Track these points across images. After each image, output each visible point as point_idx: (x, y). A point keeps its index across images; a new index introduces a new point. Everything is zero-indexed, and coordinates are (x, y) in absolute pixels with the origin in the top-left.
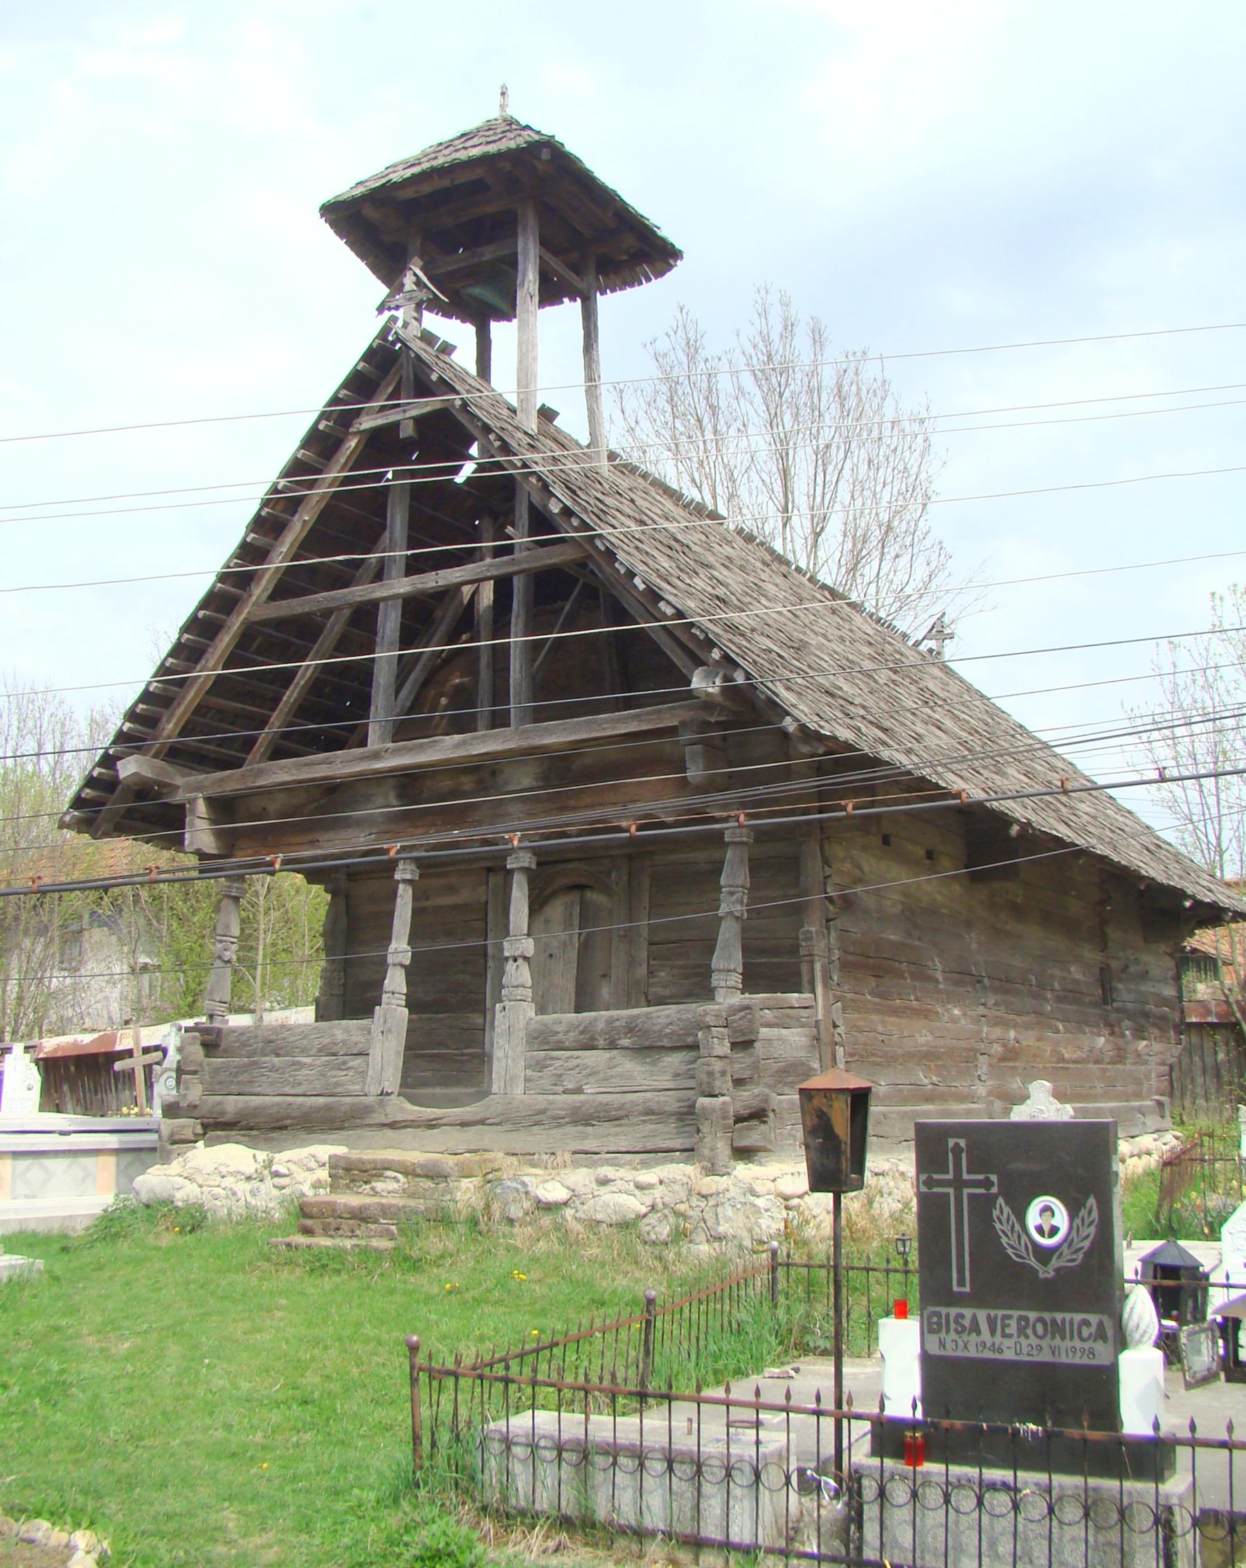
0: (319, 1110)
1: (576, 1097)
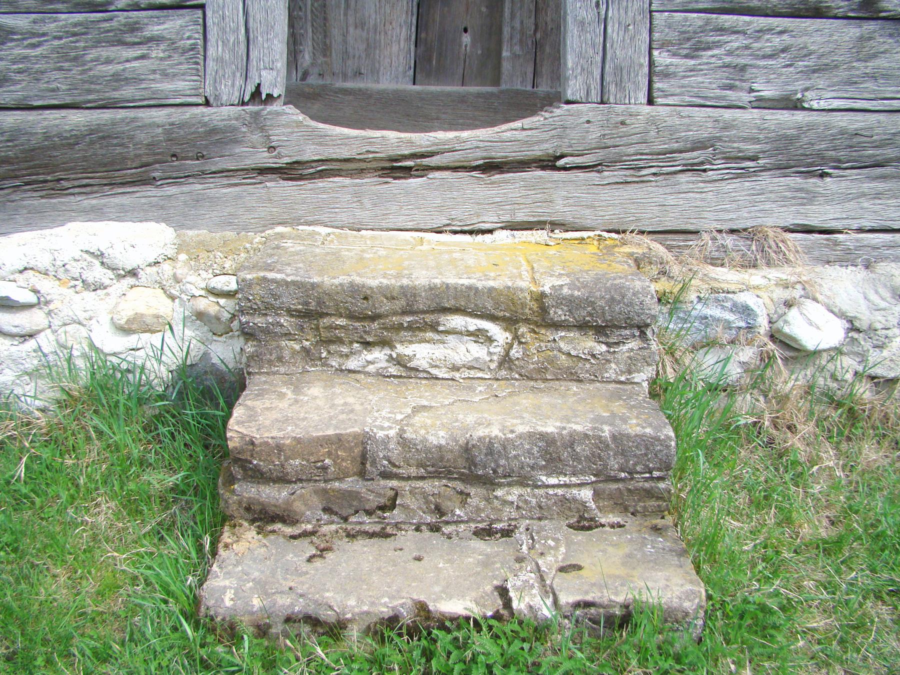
0: (72, 141)
1: (784, 116)
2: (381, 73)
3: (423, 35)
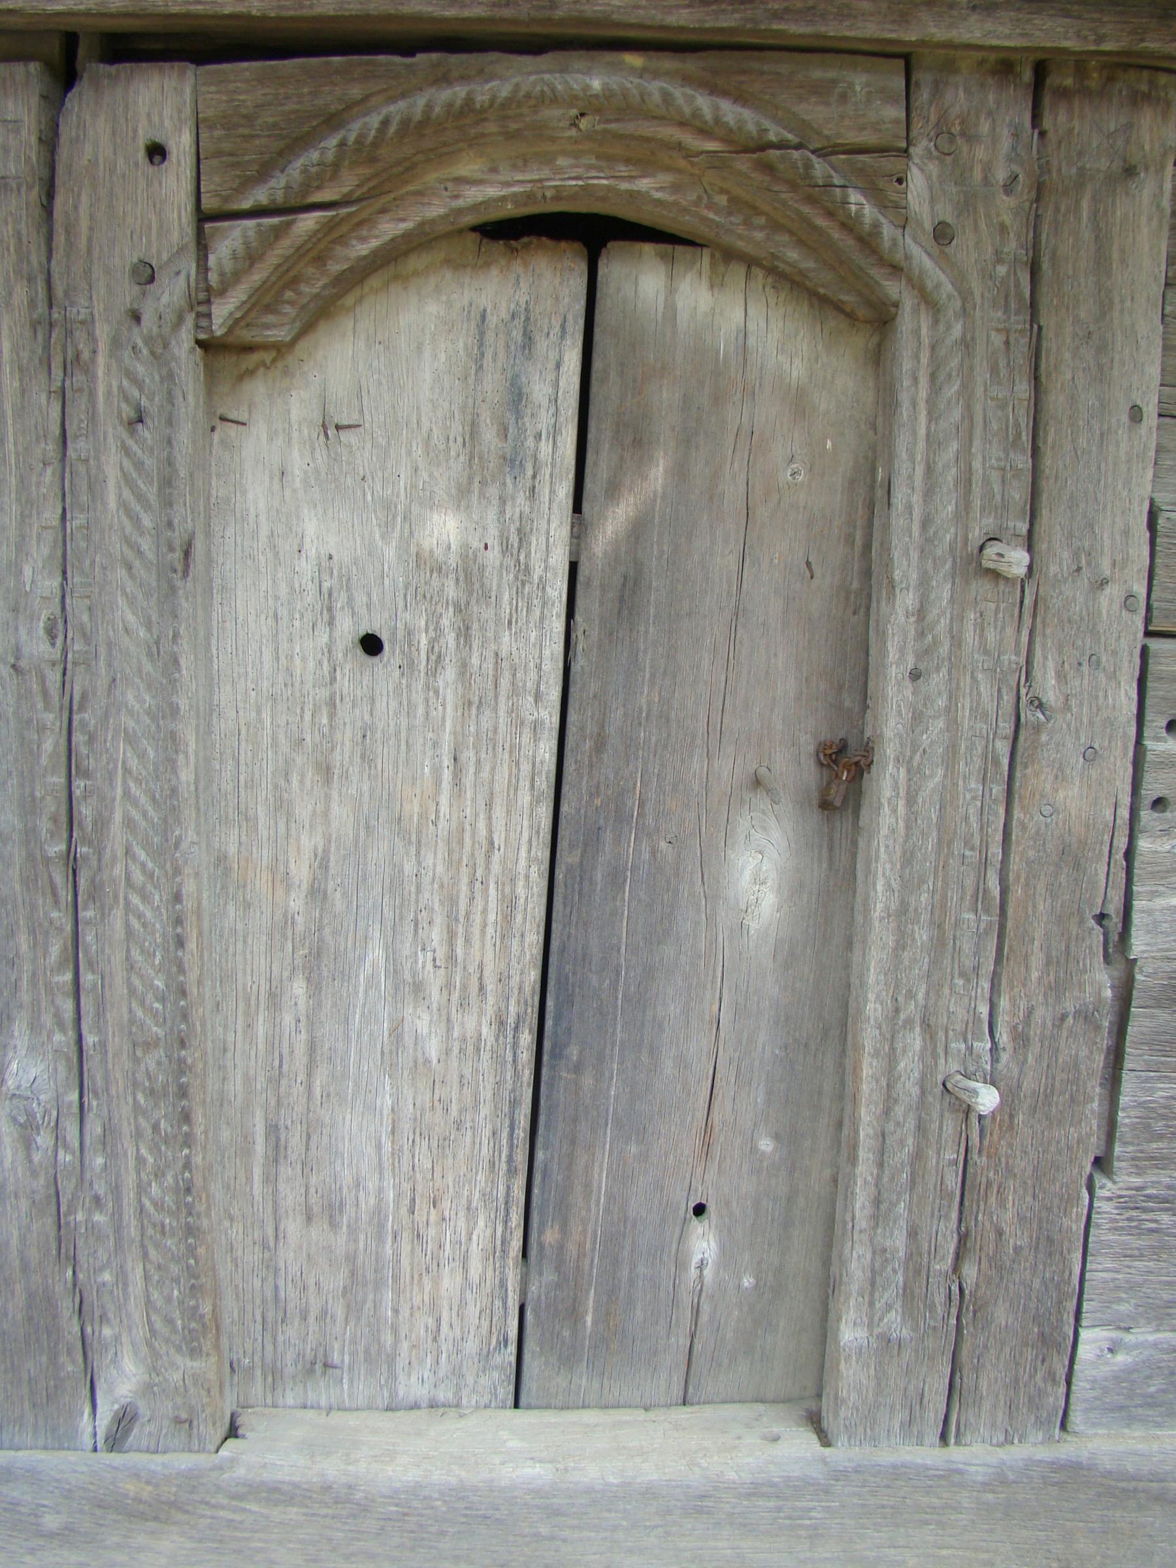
2: (401, 1362)
3: (551, 1236)
